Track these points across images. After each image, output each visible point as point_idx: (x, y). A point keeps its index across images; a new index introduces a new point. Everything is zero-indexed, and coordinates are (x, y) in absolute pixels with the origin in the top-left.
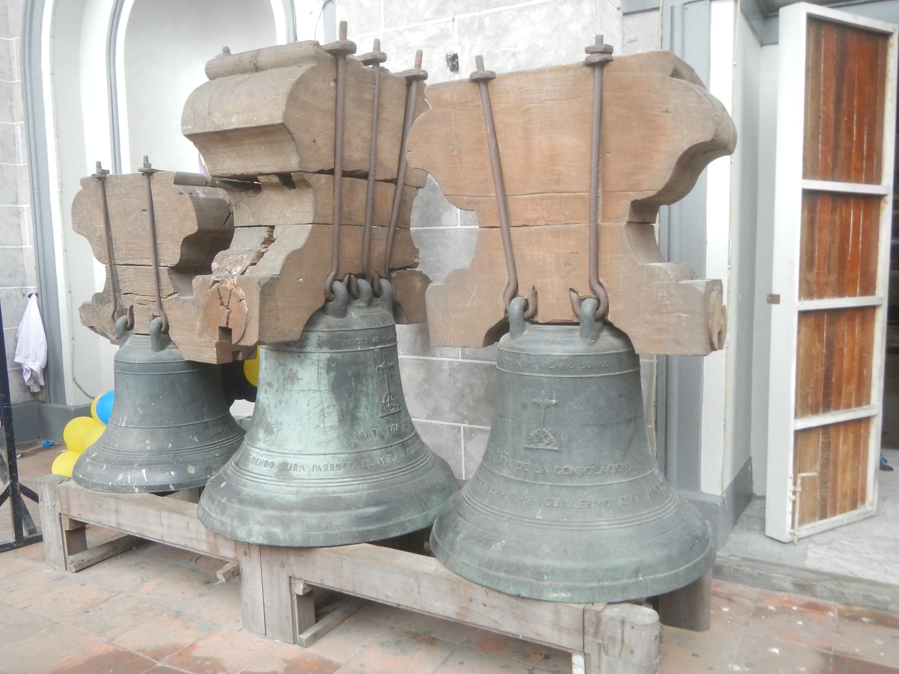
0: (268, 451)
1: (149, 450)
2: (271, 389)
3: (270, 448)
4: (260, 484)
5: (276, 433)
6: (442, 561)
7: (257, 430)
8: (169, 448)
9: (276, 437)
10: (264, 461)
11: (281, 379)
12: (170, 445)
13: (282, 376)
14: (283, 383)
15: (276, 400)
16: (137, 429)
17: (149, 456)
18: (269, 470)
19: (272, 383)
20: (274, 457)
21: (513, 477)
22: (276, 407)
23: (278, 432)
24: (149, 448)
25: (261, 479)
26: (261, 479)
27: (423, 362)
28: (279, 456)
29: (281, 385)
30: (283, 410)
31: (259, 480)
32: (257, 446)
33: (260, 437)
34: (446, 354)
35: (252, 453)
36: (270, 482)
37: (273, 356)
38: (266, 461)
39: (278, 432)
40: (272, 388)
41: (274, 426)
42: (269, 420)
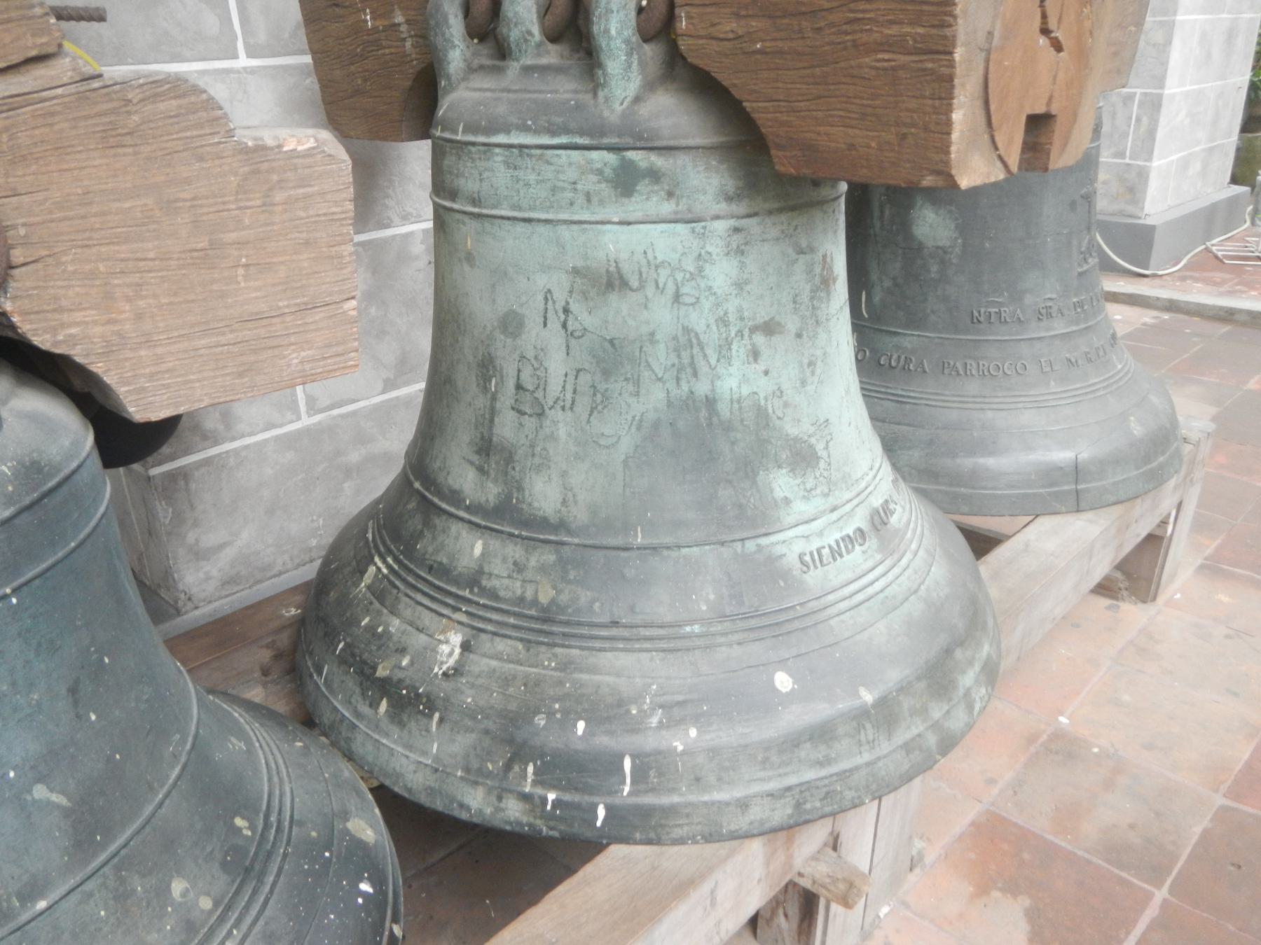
0: (833, 510)
1: (216, 904)
2: (776, 339)
3: (832, 501)
4: (882, 596)
5: (825, 454)
6: (1063, 509)
7: (754, 483)
8: (249, 833)
9: (829, 464)
10: (837, 542)
11: (805, 297)
12: (239, 822)
13: (808, 287)
14: (813, 308)
15: (801, 365)
16: (89, 886)
17: (244, 927)
18: (863, 552)
19: (777, 318)
20: (850, 514)
21: (1074, 328)
22: (804, 383)
23: (827, 448)
24: (206, 903)
25: (872, 583)
26: (872, 583)
27: (360, 249)
28: (857, 506)
29: (808, 314)
30: (822, 382)
31: (870, 591)
32: (790, 520)
33: (779, 494)
34: (414, 213)
35: (780, 550)
36: (890, 576)
37: (774, 232)
38: (843, 539)
39: (827, 448)
40: (780, 333)
41: (813, 440)
42: (792, 430)
